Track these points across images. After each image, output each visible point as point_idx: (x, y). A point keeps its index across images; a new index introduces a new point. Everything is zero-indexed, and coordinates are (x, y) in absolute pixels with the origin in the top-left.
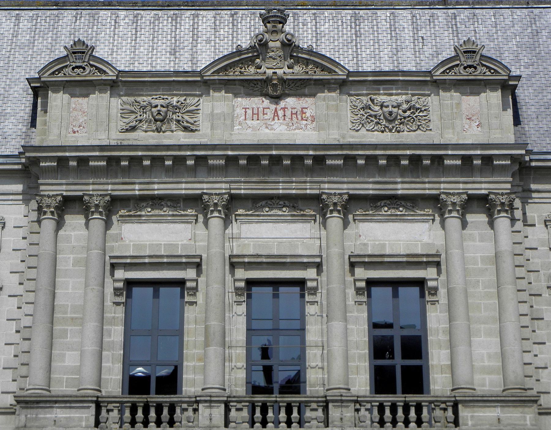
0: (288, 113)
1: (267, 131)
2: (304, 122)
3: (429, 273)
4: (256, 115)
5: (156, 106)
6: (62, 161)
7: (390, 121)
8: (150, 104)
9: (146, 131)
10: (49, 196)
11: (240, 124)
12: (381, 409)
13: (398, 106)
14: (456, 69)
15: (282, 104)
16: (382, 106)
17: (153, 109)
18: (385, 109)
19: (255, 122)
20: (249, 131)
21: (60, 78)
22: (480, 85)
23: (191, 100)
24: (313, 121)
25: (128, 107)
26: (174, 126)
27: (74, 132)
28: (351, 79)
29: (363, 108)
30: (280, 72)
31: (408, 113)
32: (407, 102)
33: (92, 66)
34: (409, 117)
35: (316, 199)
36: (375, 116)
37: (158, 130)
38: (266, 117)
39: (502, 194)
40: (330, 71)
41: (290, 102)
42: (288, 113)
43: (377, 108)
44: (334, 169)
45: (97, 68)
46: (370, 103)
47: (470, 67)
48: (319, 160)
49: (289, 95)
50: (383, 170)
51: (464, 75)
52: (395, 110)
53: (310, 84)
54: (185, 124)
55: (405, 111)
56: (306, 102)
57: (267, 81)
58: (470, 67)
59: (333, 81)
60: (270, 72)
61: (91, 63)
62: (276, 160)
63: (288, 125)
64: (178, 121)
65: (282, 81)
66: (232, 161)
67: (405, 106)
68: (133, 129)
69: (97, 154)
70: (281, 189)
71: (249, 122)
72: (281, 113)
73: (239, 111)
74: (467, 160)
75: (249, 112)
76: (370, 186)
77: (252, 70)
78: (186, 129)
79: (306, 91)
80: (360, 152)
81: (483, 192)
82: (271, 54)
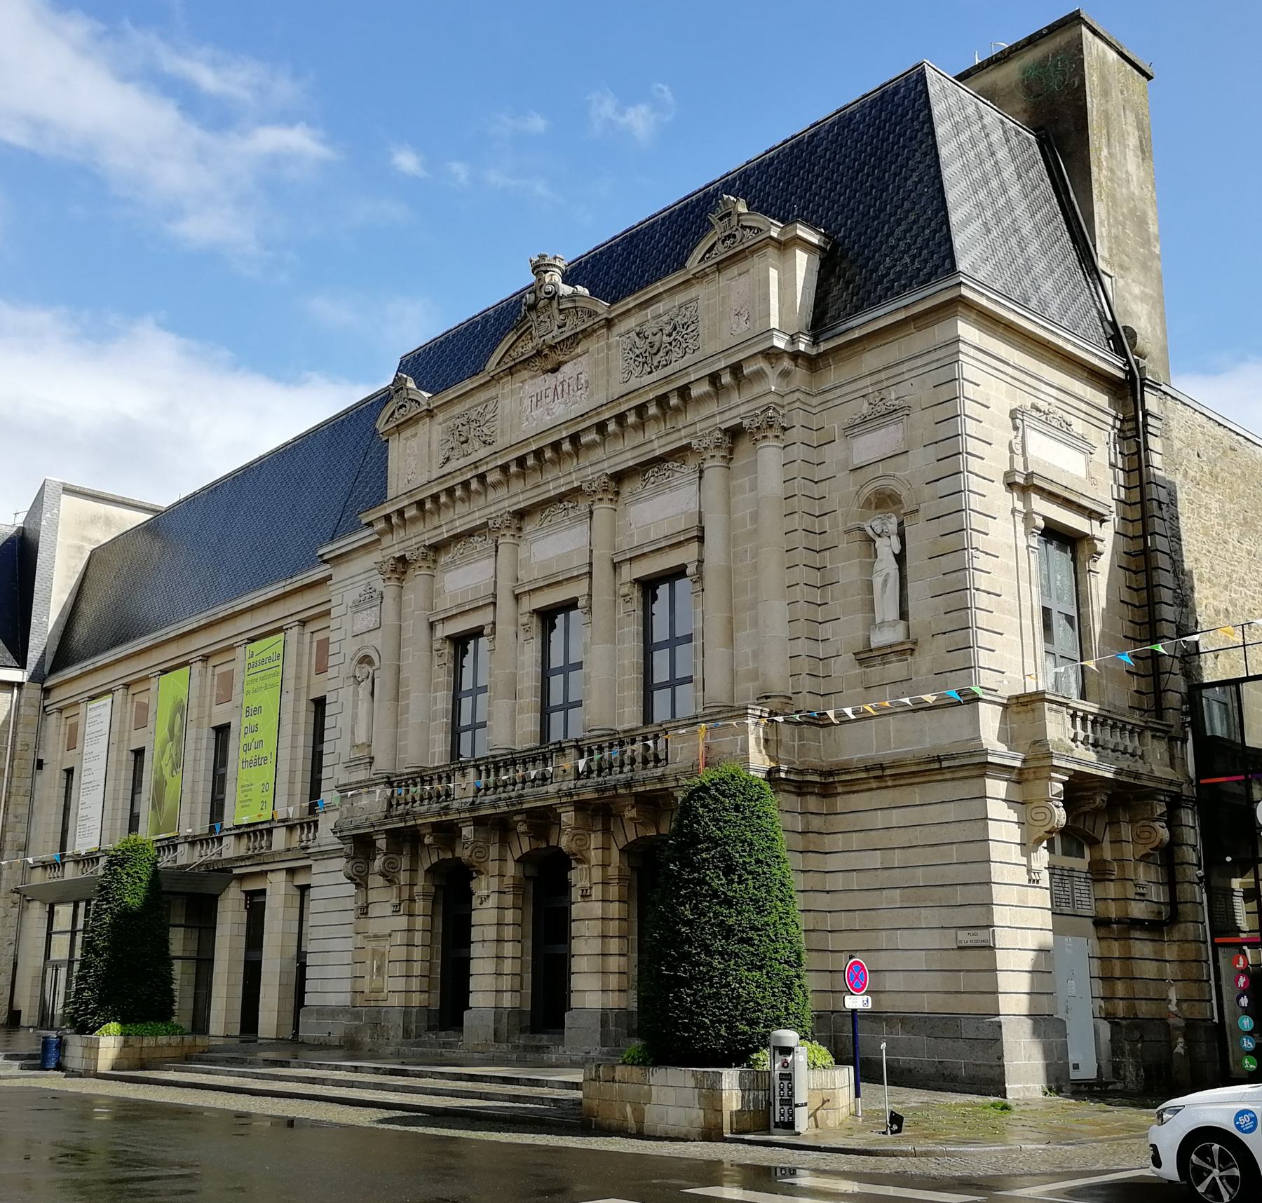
22: (746, 257)
34: (675, 340)
44: (592, 446)
48: (574, 438)
53: (580, 340)
55: (670, 335)
59: (596, 326)
61: (411, 397)
63: (566, 403)
67: (668, 329)
68: (448, 459)
76: (628, 455)
79: (579, 350)
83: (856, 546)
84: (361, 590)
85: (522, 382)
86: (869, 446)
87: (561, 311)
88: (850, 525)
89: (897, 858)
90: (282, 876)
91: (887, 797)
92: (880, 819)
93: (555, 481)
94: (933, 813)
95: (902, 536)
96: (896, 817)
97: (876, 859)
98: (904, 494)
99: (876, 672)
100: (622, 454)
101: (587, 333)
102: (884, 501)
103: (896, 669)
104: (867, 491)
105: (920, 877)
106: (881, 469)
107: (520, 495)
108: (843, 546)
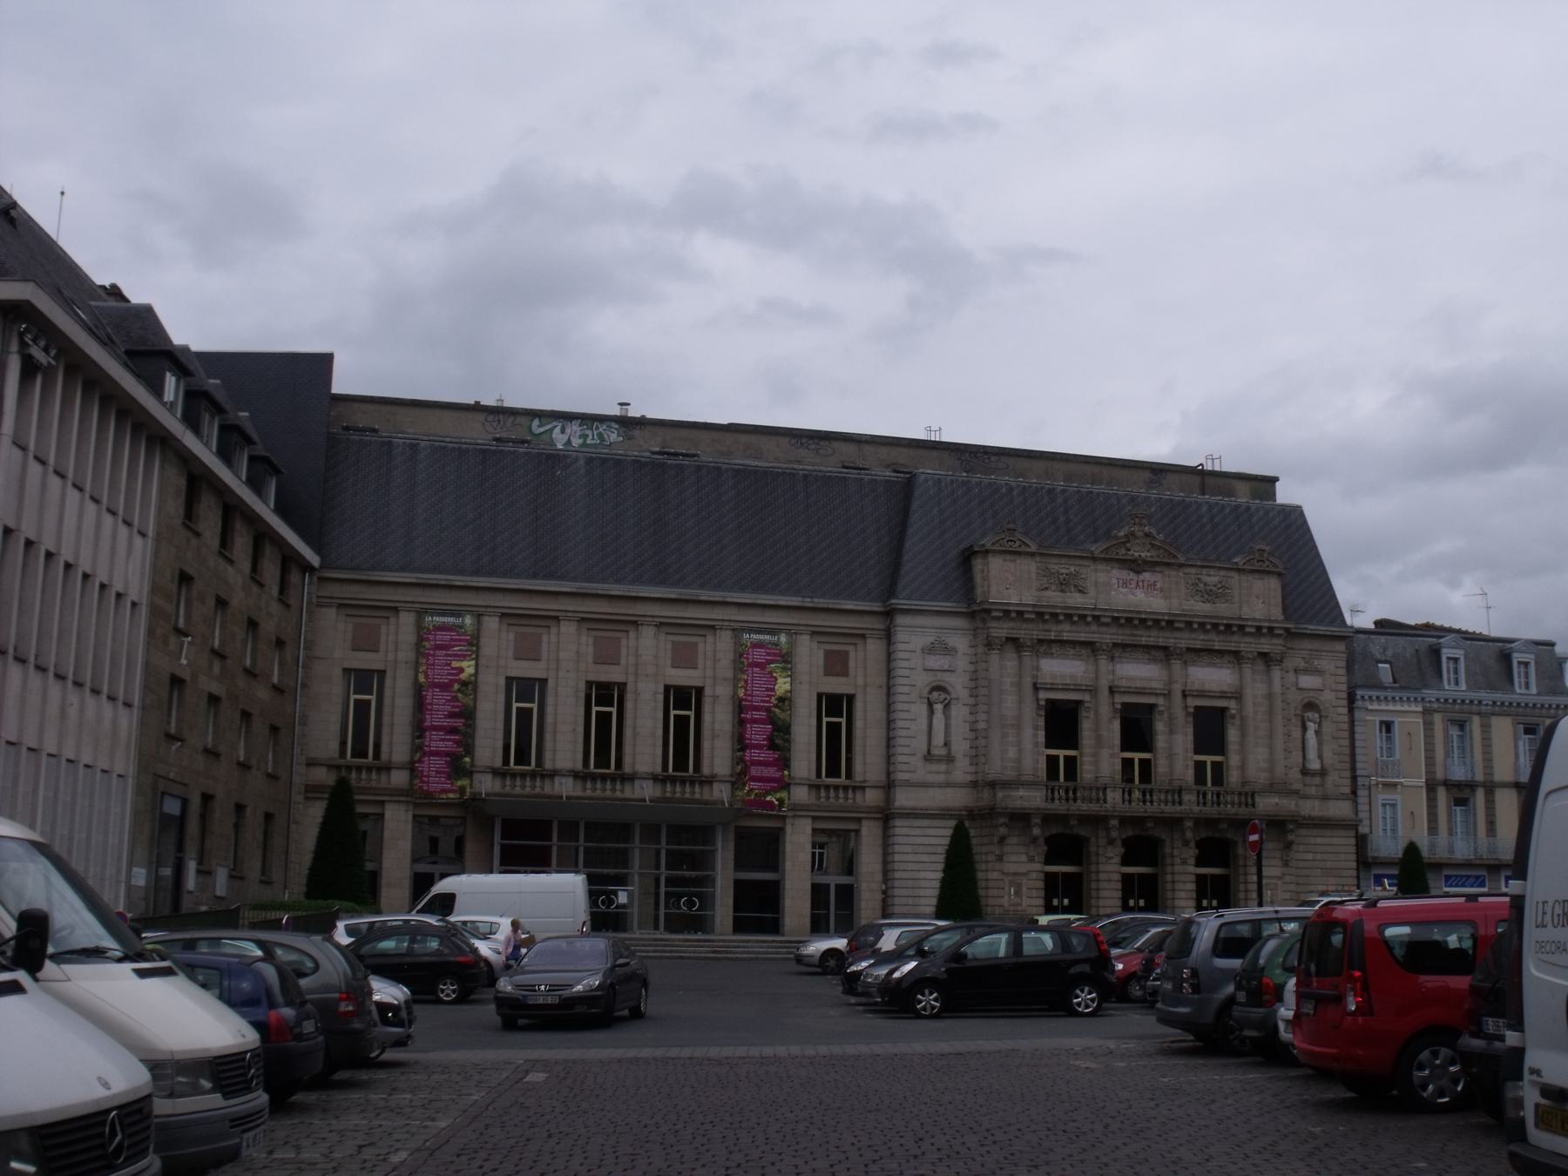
0: (1146, 584)
1: (1132, 597)
2: (1155, 592)
3: (1232, 704)
4: (1125, 584)
5: (1062, 574)
6: (1007, 613)
7: (1210, 595)
8: (1058, 573)
9: (1054, 591)
10: (997, 638)
11: (1115, 590)
12: (1198, 792)
13: (1215, 586)
14: (1252, 561)
15: (1141, 577)
16: (1205, 584)
17: (1061, 576)
18: (1208, 588)
19: (1125, 590)
20: (1121, 596)
21: (997, 547)
23: (1083, 570)
24: (1162, 591)
25: (1040, 572)
26: (1073, 590)
27: (1007, 589)
28: (1187, 563)
29: (1193, 585)
30: (1143, 555)
31: (1220, 591)
32: (1220, 582)
33: (1020, 540)
35: (1165, 648)
36: (1201, 591)
37: (1062, 591)
38: (1132, 586)
39: (1277, 654)
40: (1174, 556)
41: (1147, 576)
42: (1146, 584)
43: (1202, 585)
45: (1024, 542)
46: (1197, 581)
47: (1261, 561)
48: (1170, 623)
49: (1145, 571)
50: (1207, 632)
51: (1257, 566)
52: (1214, 588)
54: (1080, 588)
56: (1157, 577)
57: (1134, 561)
58: (1261, 561)
60: (1137, 554)
62: (1143, 621)
64: (1075, 586)
65: (1145, 561)
66: (1116, 619)
67: (1219, 586)
68: (1046, 588)
69: (1030, 609)
70: (1144, 640)
71: (1120, 589)
72: (1141, 584)
73: (1115, 581)
74: (1259, 628)
75: (1121, 581)
77: (1123, 551)
78: (1080, 591)
79: (1158, 569)
80: (1196, 620)
81: (1266, 651)
82: (1138, 541)
83: (1299, 723)
84: (931, 639)
85: (1113, 568)
86: (1307, 681)
87: (1150, 544)
88: (1298, 712)
89: (1319, 856)
90: (809, 821)
91: (1316, 832)
92: (1312, 840)
93: (1146, 637)
94: (1335, 841)
95: (1320, 724)
96: (1319, 840)
97: (1310, 856)
98: (1322, 707)
99: (1308, 780)
100: (1198, 641)
101: (1168, 565)
102: (1311, 706)
103: (1317, 780)
104: (1306, 701)
105: (1329, 864)
106: (1311, 694)
107: (1121, 635)
108: (1294, 720)
